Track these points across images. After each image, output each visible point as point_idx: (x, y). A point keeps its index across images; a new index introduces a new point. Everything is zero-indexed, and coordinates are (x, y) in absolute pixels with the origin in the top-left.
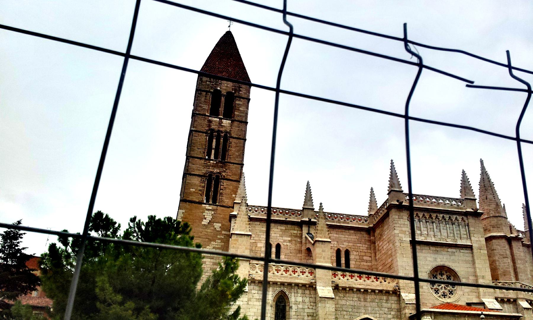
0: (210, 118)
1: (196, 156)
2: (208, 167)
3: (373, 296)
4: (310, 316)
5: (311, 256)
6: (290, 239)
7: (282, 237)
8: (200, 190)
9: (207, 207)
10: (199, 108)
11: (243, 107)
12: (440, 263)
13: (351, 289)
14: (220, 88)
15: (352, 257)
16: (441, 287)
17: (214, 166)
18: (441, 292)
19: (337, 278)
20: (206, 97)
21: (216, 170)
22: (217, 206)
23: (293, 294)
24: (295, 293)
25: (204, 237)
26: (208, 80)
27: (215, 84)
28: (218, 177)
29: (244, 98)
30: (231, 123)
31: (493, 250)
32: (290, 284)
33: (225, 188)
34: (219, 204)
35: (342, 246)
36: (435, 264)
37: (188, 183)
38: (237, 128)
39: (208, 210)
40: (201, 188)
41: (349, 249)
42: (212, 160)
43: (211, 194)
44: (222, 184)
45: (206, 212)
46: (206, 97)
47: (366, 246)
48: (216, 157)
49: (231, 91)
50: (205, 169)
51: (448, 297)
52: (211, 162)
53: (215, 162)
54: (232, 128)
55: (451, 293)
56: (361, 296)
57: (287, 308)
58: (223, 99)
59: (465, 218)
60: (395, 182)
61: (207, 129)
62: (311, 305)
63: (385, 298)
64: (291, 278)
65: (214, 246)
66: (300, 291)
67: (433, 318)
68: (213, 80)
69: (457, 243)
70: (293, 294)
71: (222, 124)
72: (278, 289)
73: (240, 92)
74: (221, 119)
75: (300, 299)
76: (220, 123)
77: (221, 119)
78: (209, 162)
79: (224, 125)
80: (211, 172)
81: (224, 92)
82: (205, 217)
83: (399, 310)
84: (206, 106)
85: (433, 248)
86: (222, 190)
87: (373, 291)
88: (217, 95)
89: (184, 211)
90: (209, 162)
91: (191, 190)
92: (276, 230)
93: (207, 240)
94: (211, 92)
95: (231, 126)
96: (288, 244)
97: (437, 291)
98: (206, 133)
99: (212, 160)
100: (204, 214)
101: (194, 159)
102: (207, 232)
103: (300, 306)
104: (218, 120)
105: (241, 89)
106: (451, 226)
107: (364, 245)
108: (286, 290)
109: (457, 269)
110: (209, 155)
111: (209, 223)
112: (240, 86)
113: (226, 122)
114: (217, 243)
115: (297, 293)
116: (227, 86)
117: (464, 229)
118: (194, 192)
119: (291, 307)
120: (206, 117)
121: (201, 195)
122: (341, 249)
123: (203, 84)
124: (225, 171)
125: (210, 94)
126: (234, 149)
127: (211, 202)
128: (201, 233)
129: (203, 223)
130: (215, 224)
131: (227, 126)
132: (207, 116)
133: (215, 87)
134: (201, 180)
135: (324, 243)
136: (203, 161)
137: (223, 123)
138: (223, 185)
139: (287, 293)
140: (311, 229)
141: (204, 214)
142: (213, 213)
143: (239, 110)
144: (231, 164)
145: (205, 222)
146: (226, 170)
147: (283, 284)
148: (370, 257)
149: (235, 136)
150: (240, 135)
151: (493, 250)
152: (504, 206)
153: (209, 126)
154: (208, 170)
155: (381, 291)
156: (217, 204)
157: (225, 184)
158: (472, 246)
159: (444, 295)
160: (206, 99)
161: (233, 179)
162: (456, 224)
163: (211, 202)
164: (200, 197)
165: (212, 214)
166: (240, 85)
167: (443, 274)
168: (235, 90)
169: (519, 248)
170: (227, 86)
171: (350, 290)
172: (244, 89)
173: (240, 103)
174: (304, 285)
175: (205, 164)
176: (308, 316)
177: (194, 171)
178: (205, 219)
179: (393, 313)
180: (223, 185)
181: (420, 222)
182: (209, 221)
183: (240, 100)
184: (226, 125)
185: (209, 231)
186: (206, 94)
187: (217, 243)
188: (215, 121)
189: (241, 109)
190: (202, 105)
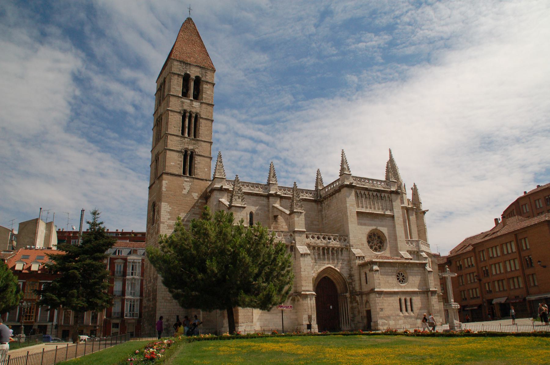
0: (183, 100)
1: (173, 133)
5: (277, 222)
11: (210, 91)
14: (189, 71)
16: (374, 244)
17: (189, 143)
18: (374, 247)
20: (178, 79)
21: (191, 147)
22: (193, 178)
25: (185, 204)
27: (185, 68)
28: (192, 153)
29: (210, 83)
33: (198, 163)
37: (169, 157)
39: (186, 181)
40: (179, 163)
42: (187, 138)
45: (185, 183)
46: (178, 79)
50: (182, 146)
54: (201, 110)
58: (192, 84)
59: (390, 195)
60: (345, 166)
61: (180, 109)
65: (194, 212)
71: (193, 106)
73: (207, 77)
74: (191, 100)
76: (191, 105)
77: (191, 100)
79: (194, 106)
80: (187, 148)
81: (193, 77)
83: (349, 261)
84: (178, 88)
88: (186, 78)
89: (167, 182)
91: (171, 163)
92: (249, 201)
94: (182, 75)
95: (200, 107)
97: (371, 247)
98: (180, 113)
102: (187, 200)
105: (207, 74)
106: (381, 201)
110: (183, 133)
111: (188, 193)
113: (196, 104)
114: (195, 210)
117: (389, 203)
118: (174, 166)
121: (180, 168)
127: (188, 175)
129: (183, 193)
130: (193, 194)
132: (180, 97)
133: (185, 71)
136: (179, 139)
138: (197, 160)
141: (183, 185)
142: (190, 184)
143: (207, 93)
145: (185, 192)
149: (204, 117)
150: (208, 116)
152: (405, 185)
153: (182, 106)
156: (193, 176)
158: (394, 215)
160: (178, 81)
161: (205, 155)
162: (384, 199)
164: (179, 170)
165: (190, 185)
168: (202, 74)
177: (172, 147)
178: (185, 189)
179: (345, 263)
180: (197, 160)
181: (362, 197)
184: (196, 106)
185: (188, 199)
187: (195, 210)
189: (207, 92)
190: (175, 87)
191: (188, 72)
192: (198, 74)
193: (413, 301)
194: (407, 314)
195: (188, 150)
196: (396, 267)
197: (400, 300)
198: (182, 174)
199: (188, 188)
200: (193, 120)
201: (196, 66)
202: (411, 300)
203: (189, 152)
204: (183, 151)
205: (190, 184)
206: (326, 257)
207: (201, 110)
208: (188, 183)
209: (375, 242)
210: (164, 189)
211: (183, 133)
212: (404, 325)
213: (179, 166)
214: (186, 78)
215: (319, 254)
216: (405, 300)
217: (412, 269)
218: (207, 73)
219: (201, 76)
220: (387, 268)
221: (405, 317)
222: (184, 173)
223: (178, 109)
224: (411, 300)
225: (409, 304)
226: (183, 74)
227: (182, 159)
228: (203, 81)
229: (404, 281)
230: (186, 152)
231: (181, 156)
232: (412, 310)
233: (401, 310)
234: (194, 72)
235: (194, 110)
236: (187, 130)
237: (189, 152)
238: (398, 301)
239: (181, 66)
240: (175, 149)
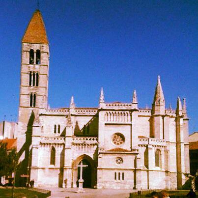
9: (31, 108)
21: (34, 91)
48: (34, 85)
55: (121, 143)
58: (35, 54)
72: (51, 146)
76: (34, 67)
81: (35, 51)
85: (115, 126)
97: (115, 143)
104: (33, 66)
108: (54, 145)
109: (124, 134)
110: (30, 84)
113: (37, 67)
127: (33, 106)
136: (27, 87)
155: (91, 144)
159: (118, 144)
163: (33, 106)
192: (38, 49)
194: (119, 181)
197: (115, 173)
200: (36, 76)
202: (123, 174)
203: (33, 94)
206: (83, 149)
209: (118, 140)
210: (20, 115)
211: (30, 84)
214: (32, 52)
215: (79, 148)
216: (119, 173)
221: (117, 183)
222: (31, 105)
223: (27, 71)
224: (123, 174)
225: (121, 176)
230: (31, 94)
232: (123, 179)
233: (115, 179)
234: (36, 47)
235: (35, 71)
236: (32, 82)
237: (33, 94)
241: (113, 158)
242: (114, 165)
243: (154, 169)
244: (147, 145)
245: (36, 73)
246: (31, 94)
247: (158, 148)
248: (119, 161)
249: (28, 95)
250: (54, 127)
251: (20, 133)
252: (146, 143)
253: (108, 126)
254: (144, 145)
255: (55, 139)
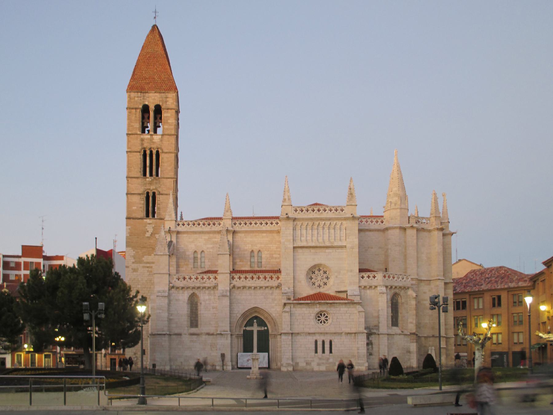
0: (142, 137)
1: (133, 176)
2: (145, 185)
3: (261, 291)
4: (215, 308)
6: (212, 246)
7: (206, 245)
8: (141, 207)
9: (148, 221)
10: (131, 128)
12: (317, 262)
13: (244, 287)
15: (263, 256)
16: (317, 280)
17: (151, 183)
18: (317, 284)
19: (235, 280)
20: (136, 114)
21: (152, 187)
22: (156, 219)
23: (202, 295)
24: (203, 294)
26: (136, 96)
27: (143, 99)
29: (171, 109)
30: (162, 138)
31: (388, 240)
32: (199, 288)
33: (161, 202)
34: (158, 218)
35: (256, 248)
36: (312, 264)
38: (168, 143)
39: (149, 224)
41: (261, 250)
43: (150, 209)
44: (158, 199)
46: (136, 114)
47: (276, 246)
48: (151, 175)
49: (159, 104)
50: (143, 188)
51: (322, 287)
52: (147, 179)
53: (151, 180)
56: (252, 291)
57: (199, 304)
58: (152, 114)
61: (140, 148)
62: (215, 301)
63: (271, 292)
64: (201, 283)
66: (207, 292)
67: (292, 306)
68: (141, 94)
69: (333, 245)
70: (202, 295)
71: (154, 141)
72: (191, 292)
73: (168, 103)
74: (152, 135)
75: (207, 297)
76: (151, 140)
77: (152, 135)
78: (145, 181)
80: (148, 189)
81: (152, 108)
82: (148, 230)
85: (313, 250)
86: (159, 204)
87: (261, 287)
88: (145, 109)
90: (145, 181)
93: (151, 249)
95: (161, 141)
96: (211, 250)
98: (140, 152)
99: (148, 178)
100: (146, 228)
101: (132, 179)
103: (207, 302)
104: (149, 136)
105: (168, 99)
107: (274, 245)
108: (196, 292)
111: (151, 235)
112: (168, 96)
115: (205, 293)
116: (154, 99)
119: (201, 304)
120: (138, 136)
122: (254, 250)
123: (133, 101)
124: (160, 187)
125: (138, 110)
126: (166, 164)
128: (146, 243)
131: (158, 142)
132: (139, 134)
134: (141, 198)
135: (224, 255)
136: (139, 181)
137: (154, 139)
138: (159, 200)
139: (197, 294)
140: (228, 236)
141: (146, 228)
143: (168, 123)
144: (164, 180)
145: (148, 235)
146: (161, 185)
147: (193, 288)
148: (278, 254)
151: (388, 240)
153: (142, 144)
154: (146, 188)
157: (161, 199)
165: (153, 227)
166: (166, 95)
167: (321, 270)
168: (162, 101)
169: (413, 236)
170: (154, 99)
171: (243, 288)
172: (171, 99)
173: (169, 115)
174: (209, 288)
175: (142, 182)
176: (213, 308)
178: (148, 231)
179: (275, 302)
180: (159, 200)
182: (151, 233)
183: (167, 112)
184: (156, 141)
185: (152, 241)
186: (136, 111)
188: (147, 139)
189: (169, 121)
190: (133, 124)
191: (147, 103)
193: (333, 343)
195: (150, 191)
196: (317, 308)
197: (316, 342)
198: (145, 217)
199: (151, 230)
201: (155, 93)
202: (331, 342)
204: (145, 193)
205: (153, 226)
207: (162, 143)
208: (151, 225)
209: (319, 278)
211: (145, 174)
212: (318, 367)
213: (141, 209)
214: (145, 109)
216: (323, 342)
217: (338, 309)
218: (167, 98)
219: (161, 104)
220: (304, 309)
221: (320, 359)
222: (147, 216)
224: (331, 342)
226: (141, 107)
227: (143, 202)
228: (164, 109)
229: (326, 322)
230: (148, 193)
231: (142, 198)
232: (331, 352)
233: (316, 352)
238: (314, 343)
239: (138, 97)
240: (137, 192)
241: (312, 311)
242: (312, 325)
243: (390, 332)
244: (376, 287)
245: (154, 152)
246: (148, 193)
247: (397, 291)
248: (323, 318)
249: (142, 194)
250: (192, 256)
251: (130, 269)
252: (374, 282)
253: (300, 251)
254: (371, 287)
255: (197, 278)
